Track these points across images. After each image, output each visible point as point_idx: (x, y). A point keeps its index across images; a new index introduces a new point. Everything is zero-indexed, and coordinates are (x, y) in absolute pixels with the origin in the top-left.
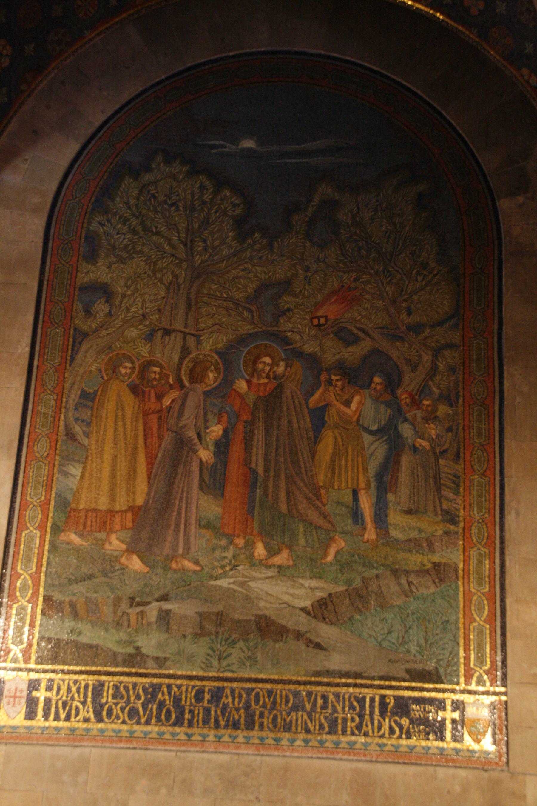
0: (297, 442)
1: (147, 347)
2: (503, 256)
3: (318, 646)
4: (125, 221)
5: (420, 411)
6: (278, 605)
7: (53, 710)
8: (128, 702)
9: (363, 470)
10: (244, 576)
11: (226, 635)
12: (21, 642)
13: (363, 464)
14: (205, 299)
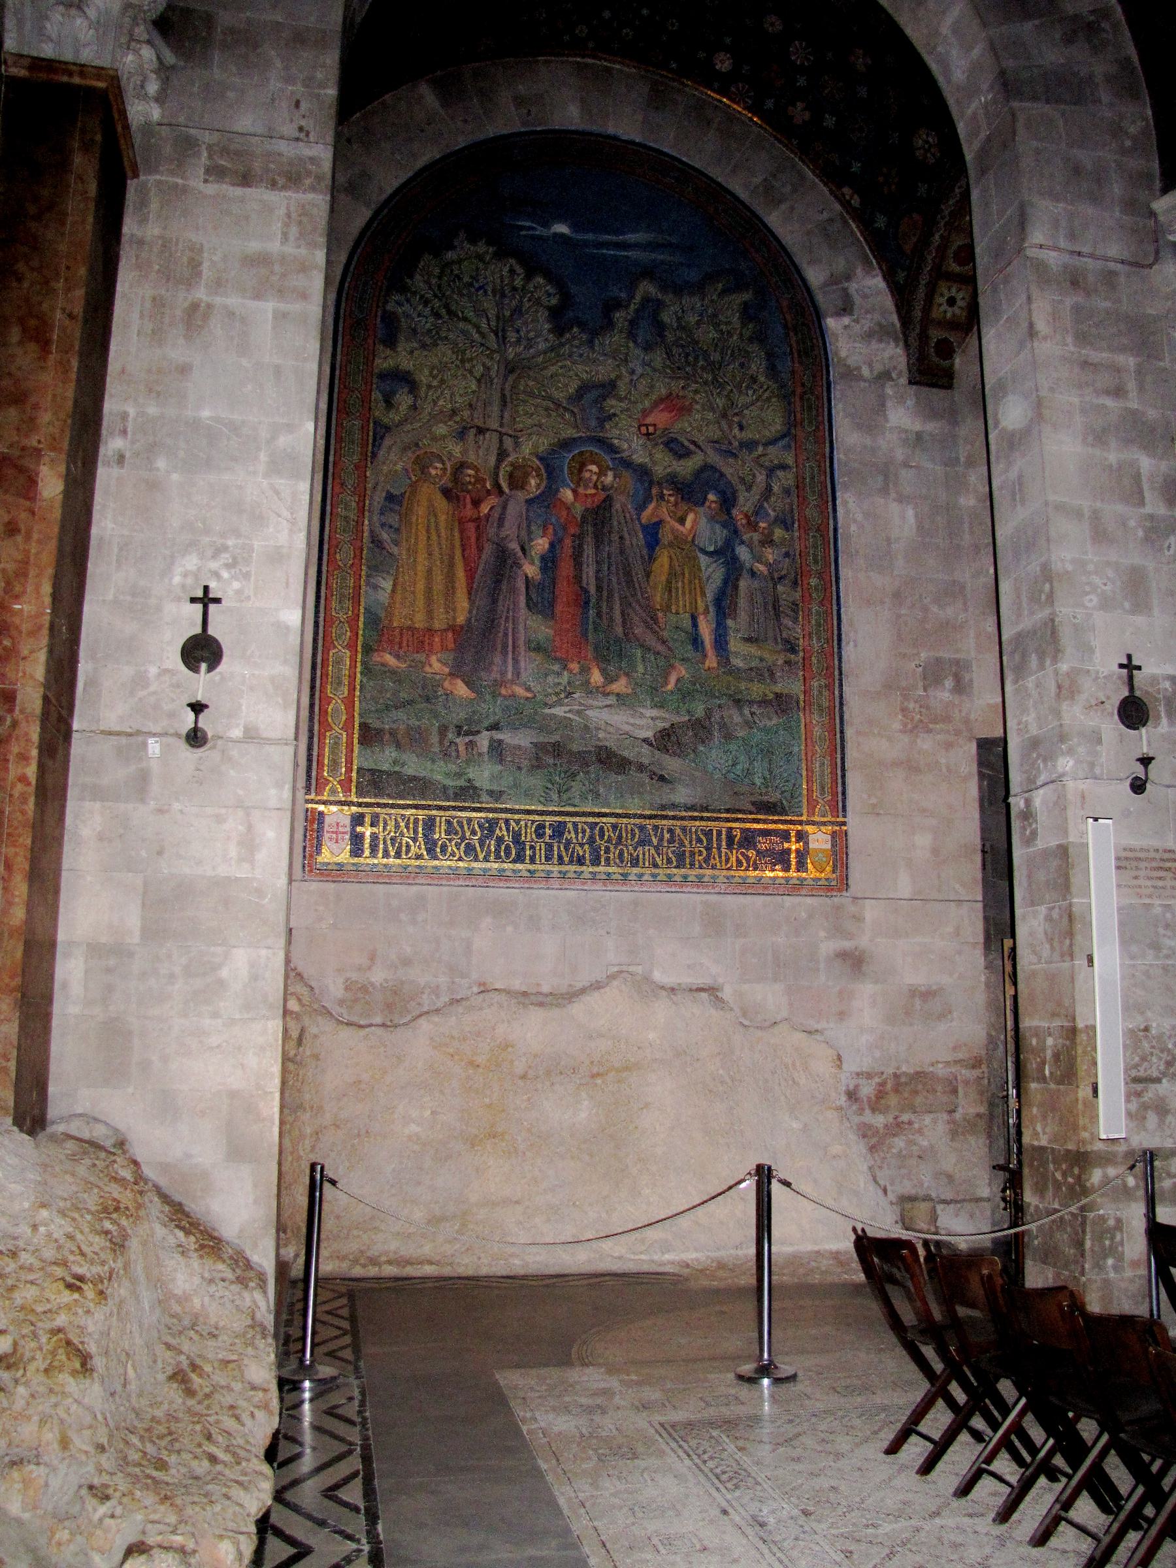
3: (662, 778)
4: (426, 303)
7: (381, 846)
8: (463, 838)
10: (581, 704)
11: (565, 767)
14: (522, 397)
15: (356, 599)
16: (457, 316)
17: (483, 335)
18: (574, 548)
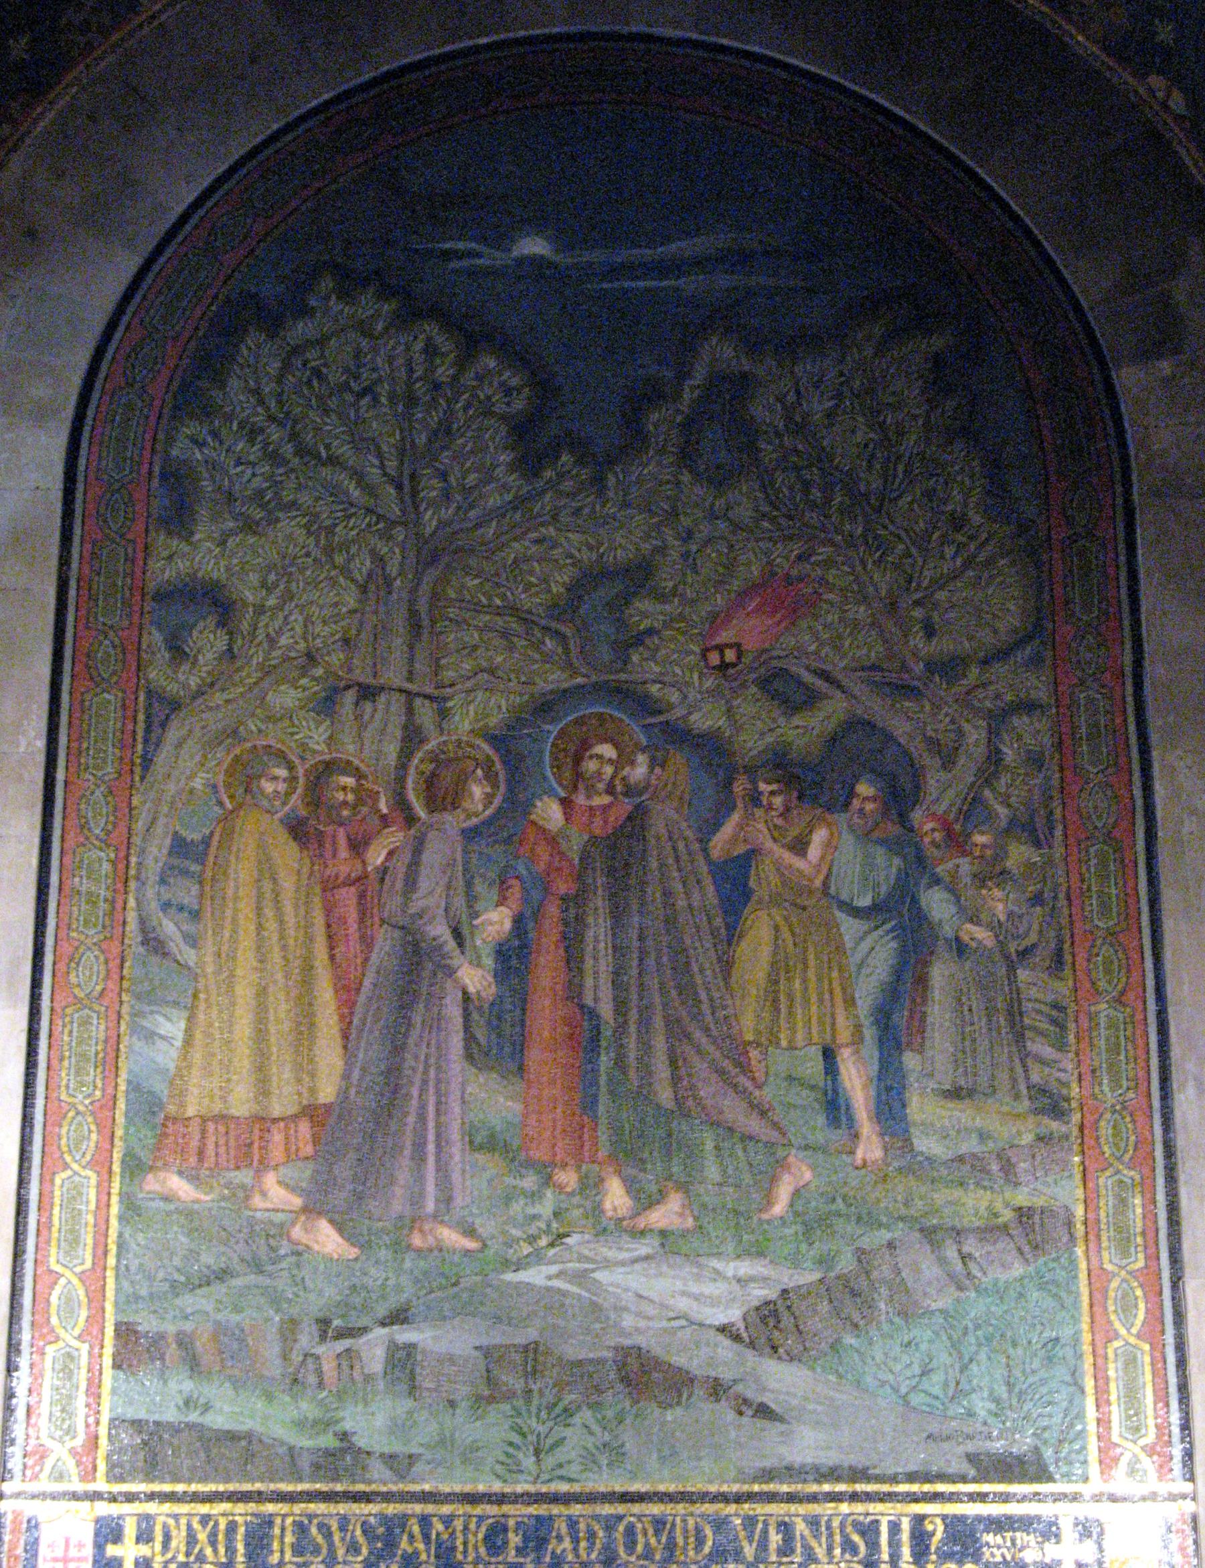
0: (688, 942)
1: (321, 730)
2: (1136, 497)
3: (764, 1411)
5: (968, 859)
9: (845, 1001)
10: (582, 1258)
11: (549, 1397)
12: (70, 1432)
13: (844, 989)
15: (110, 1061)
16: (318, 457)
17: (370, 490)
18: (566, 924)
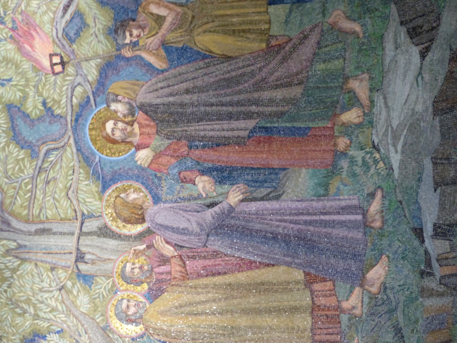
0: (212, 80)
1: (101, 282)
6: (420, 88)
14: (36, 211)
18: (204, 147)
